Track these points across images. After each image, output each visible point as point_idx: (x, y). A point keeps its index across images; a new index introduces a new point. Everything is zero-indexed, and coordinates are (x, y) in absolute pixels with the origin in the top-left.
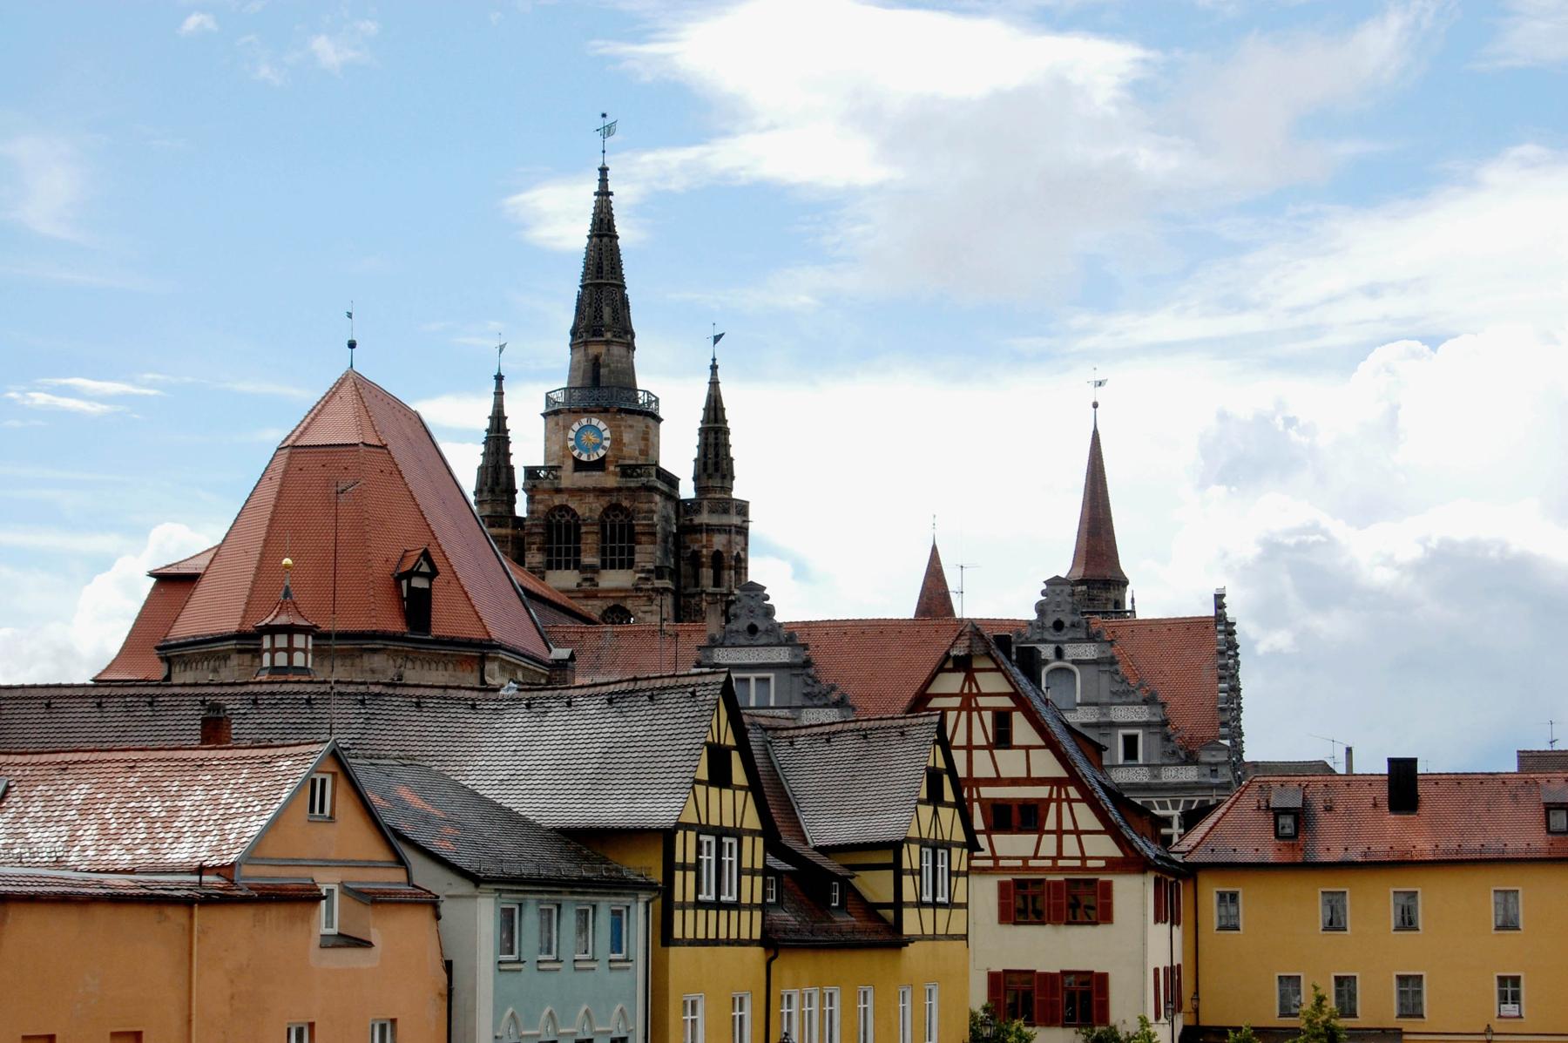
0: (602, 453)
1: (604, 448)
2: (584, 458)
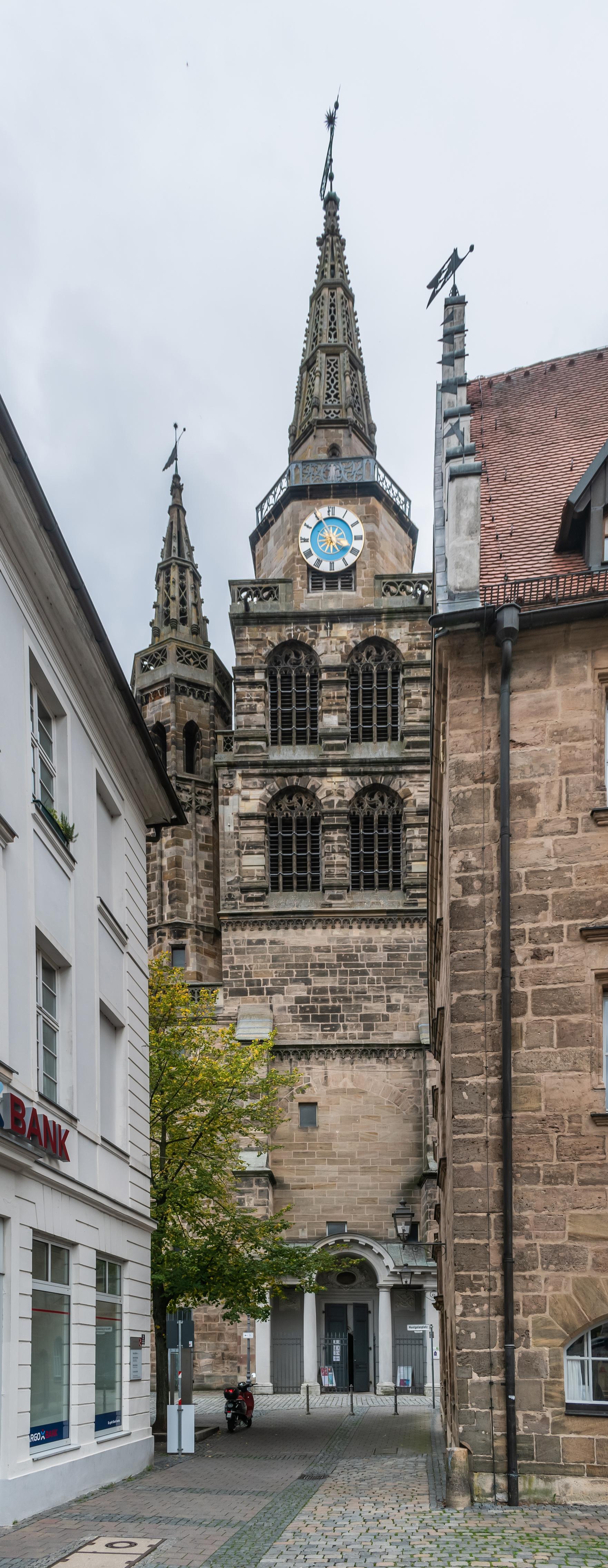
0: (351, 559)
2: (325, 567)
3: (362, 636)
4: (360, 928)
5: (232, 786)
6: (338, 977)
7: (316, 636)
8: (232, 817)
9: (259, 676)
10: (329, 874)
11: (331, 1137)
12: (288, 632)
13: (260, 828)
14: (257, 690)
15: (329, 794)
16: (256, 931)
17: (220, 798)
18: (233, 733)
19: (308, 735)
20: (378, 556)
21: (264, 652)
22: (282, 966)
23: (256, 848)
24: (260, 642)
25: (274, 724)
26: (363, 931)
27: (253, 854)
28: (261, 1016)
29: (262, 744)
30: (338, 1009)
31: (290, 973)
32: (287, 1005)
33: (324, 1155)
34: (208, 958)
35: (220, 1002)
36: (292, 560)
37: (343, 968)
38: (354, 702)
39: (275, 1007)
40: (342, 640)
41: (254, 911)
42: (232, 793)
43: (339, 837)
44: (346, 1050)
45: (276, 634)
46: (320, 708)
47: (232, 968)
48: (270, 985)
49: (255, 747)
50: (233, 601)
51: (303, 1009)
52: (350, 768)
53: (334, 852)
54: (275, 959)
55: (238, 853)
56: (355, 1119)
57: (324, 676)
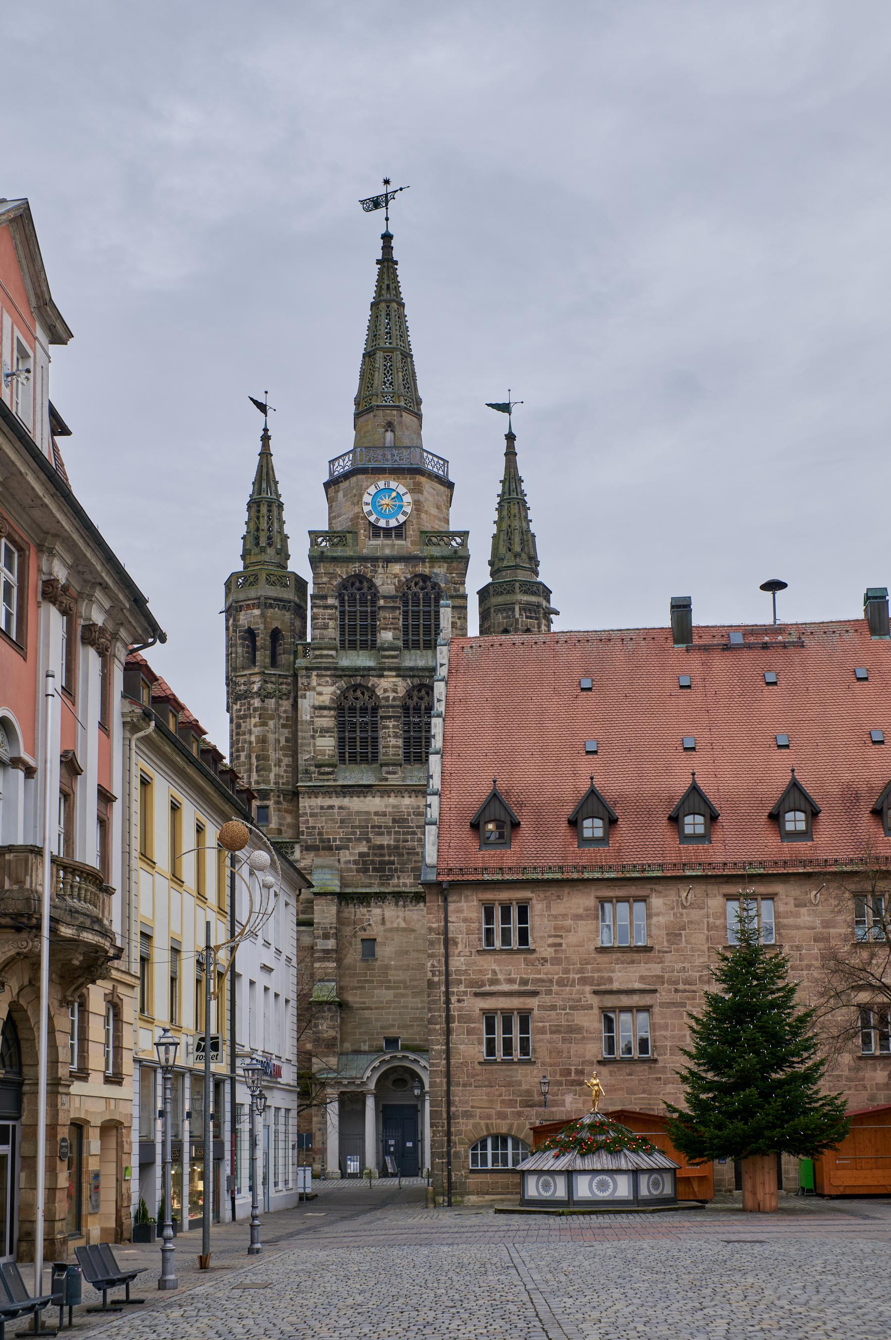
1: (405, 513)
2: (382, 523)
3: (411, 573)
4: (410, 797)
5: (309, 684)
6: (393, 836)
7: (376, 572)
8: (308, 708)
9: (330, 601)
10: (385, 754)
11: (387, 967)
12: (355, 568)
13: (331, 717)
14: (329, 611)
15: (385, 691)
16: (327, 799)
17: (300, 693)
18: (309, 644)
19: (369, 643)
20: (423, 516)
21: (335, 583)
22: (348, 827)
23: (327, 732)
24: (332, 576)
25: (342, 634)
26: (413, 799)
27: (325, 737)
28: (330, 867)
29: (333, 653)
30: (393, 863)
31: (354, 833)
32: (352, 859)
33: (382, 982)
34: (286, 815)
35: (297, 854)
36: (356, 517)
37: (397, 829)
38: (405, 619)
39: (343, 860)
40: (396, 576)
41: (326, 784)
42: (309, 690)
43: (394, 726)
44: (398, 896)
45: (344, 570)
46: (378, 623)
47: (308, 828)
48: (338, 843)
49: (327, 656)
50: (312, 545)
51: (364, 863)
52: (401, 672)
53: (389, 736)
54: (342, 821)
55: (313, 737)
56: (407, 952)
57: (382, 602)
